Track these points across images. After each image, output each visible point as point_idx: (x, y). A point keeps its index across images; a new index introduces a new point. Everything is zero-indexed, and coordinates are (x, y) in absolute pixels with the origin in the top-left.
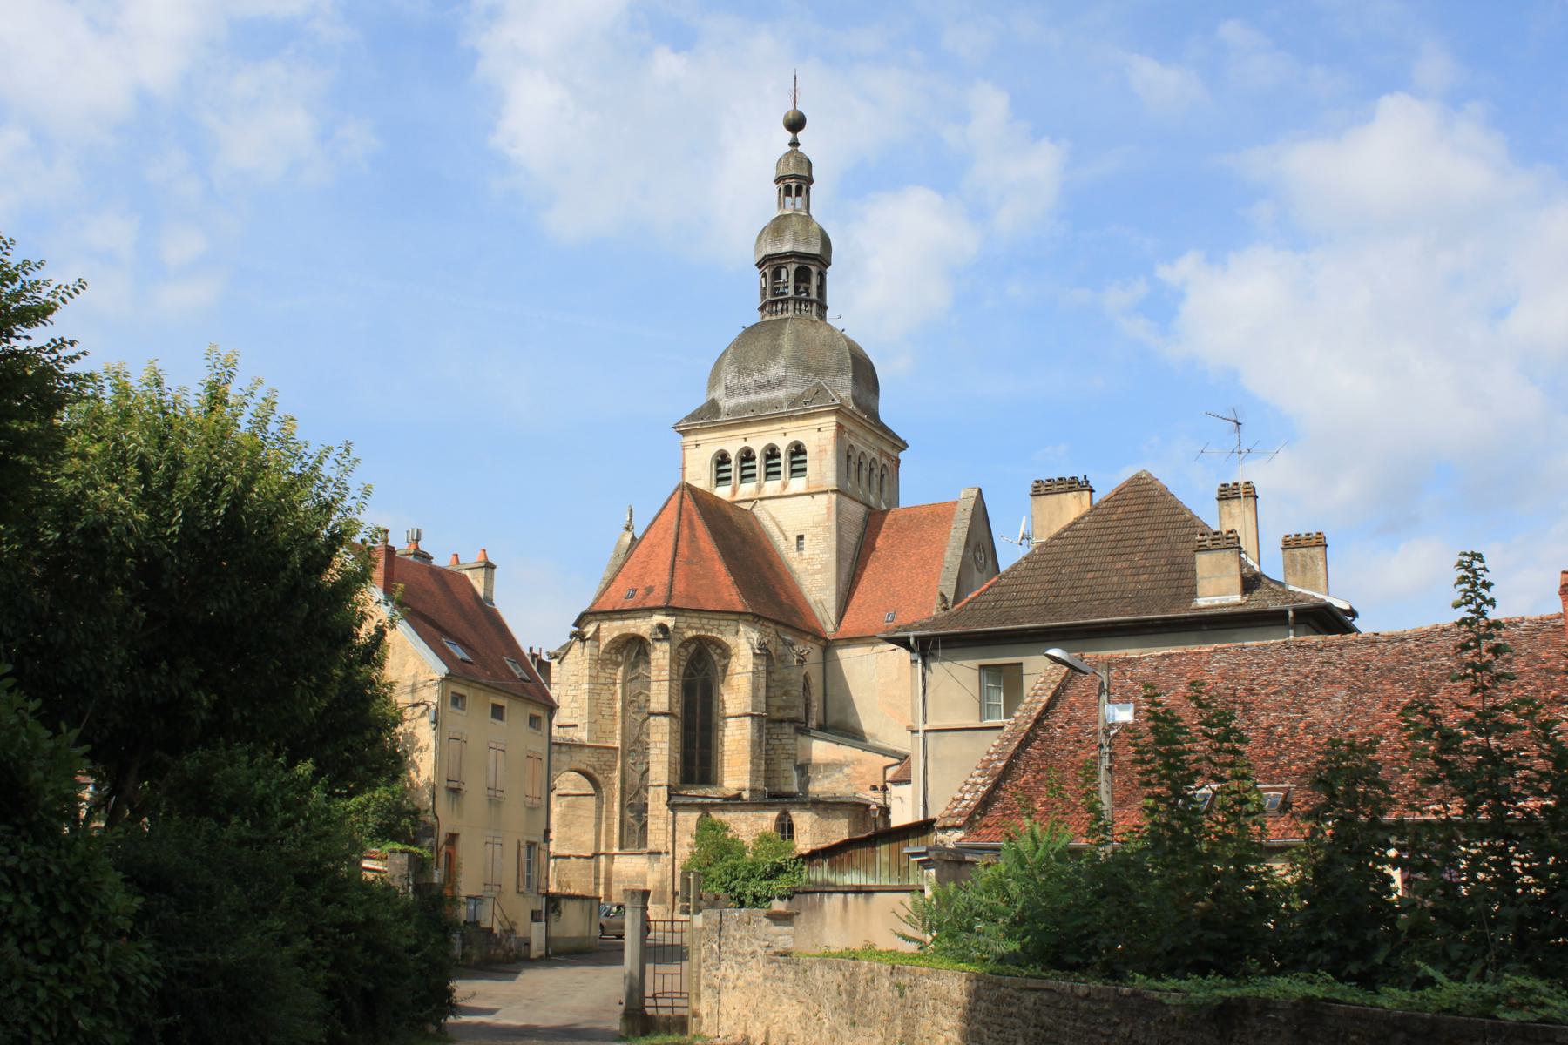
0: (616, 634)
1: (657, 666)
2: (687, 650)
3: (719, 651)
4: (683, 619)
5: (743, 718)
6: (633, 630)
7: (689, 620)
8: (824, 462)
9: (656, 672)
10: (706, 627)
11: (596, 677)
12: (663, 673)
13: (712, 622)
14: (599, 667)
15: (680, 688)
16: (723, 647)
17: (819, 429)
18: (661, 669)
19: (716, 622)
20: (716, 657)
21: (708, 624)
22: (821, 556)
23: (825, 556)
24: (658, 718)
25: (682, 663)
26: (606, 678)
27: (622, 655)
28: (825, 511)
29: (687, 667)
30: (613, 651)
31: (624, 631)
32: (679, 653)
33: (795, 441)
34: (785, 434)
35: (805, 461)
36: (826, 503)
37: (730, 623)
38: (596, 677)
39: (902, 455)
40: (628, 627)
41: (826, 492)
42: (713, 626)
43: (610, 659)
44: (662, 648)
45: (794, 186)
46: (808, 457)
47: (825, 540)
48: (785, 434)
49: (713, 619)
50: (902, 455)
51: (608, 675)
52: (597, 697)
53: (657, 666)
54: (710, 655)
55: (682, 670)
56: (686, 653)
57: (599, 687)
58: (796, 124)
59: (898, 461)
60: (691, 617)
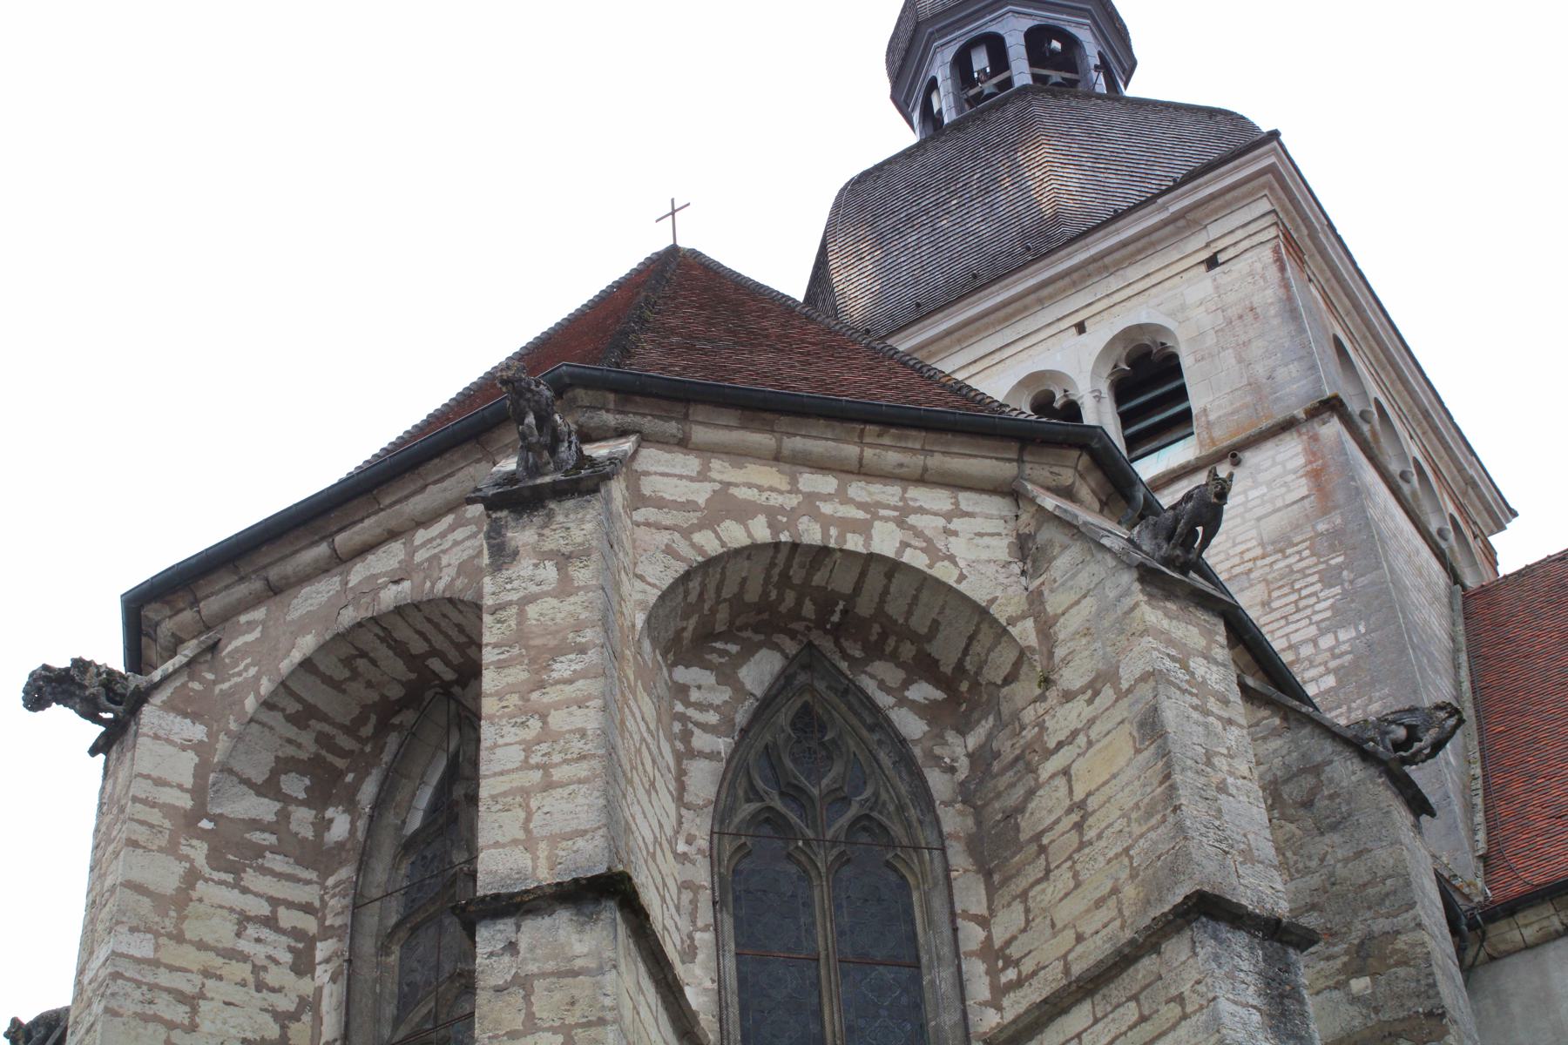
0: (306, 644)
1: (521, 636)
2: (727, 676)
3: (922, 691)
4: (689, 463)
5: (1147, 966)
6: (390, 596)
7: (721, 469)
8: (1257, 348)
9: (518, 674)
10: (826, 508)
11: (182, 899)
12: (562, 668)
13: (859, 490)
14: (198, 852)
15: (701, 874)
16: (946, 652)
17: (1212, 263)
18: (541, 659)
19: (889, 493)
20: (911, 726)
21: (842, 496)
22: (1327, 642)
23: (1344, 635)
24: (533, 932)
25: (701, 740)
26: (244, 919)
27: (351, 806)
28: (1302, 488)
29: (736, 777)
30: (295, 785)
31: (349, 617)
32: (681, 691)
33: (1127, 333)
34: (1081, 328)
35: (1181, 394)
36: (1301, 460)
37: (967, 500)
38: (182, 899)
39: (1494, 540)
40: (372, 588)
41: (1287, 426)
42: (871, 508)
43: (280, 825)
44: (554, 540)
46: (1186, 362)
47: (1329, 578)
48: (1081, 328)
49: (862, 471)
51: (263, 909)
52: (179, 1013)
53: (521, 636)
54: (880, 723)
55: (703, 780)
56: (723, 695)
57: (192, 958)
60: (739, 455)
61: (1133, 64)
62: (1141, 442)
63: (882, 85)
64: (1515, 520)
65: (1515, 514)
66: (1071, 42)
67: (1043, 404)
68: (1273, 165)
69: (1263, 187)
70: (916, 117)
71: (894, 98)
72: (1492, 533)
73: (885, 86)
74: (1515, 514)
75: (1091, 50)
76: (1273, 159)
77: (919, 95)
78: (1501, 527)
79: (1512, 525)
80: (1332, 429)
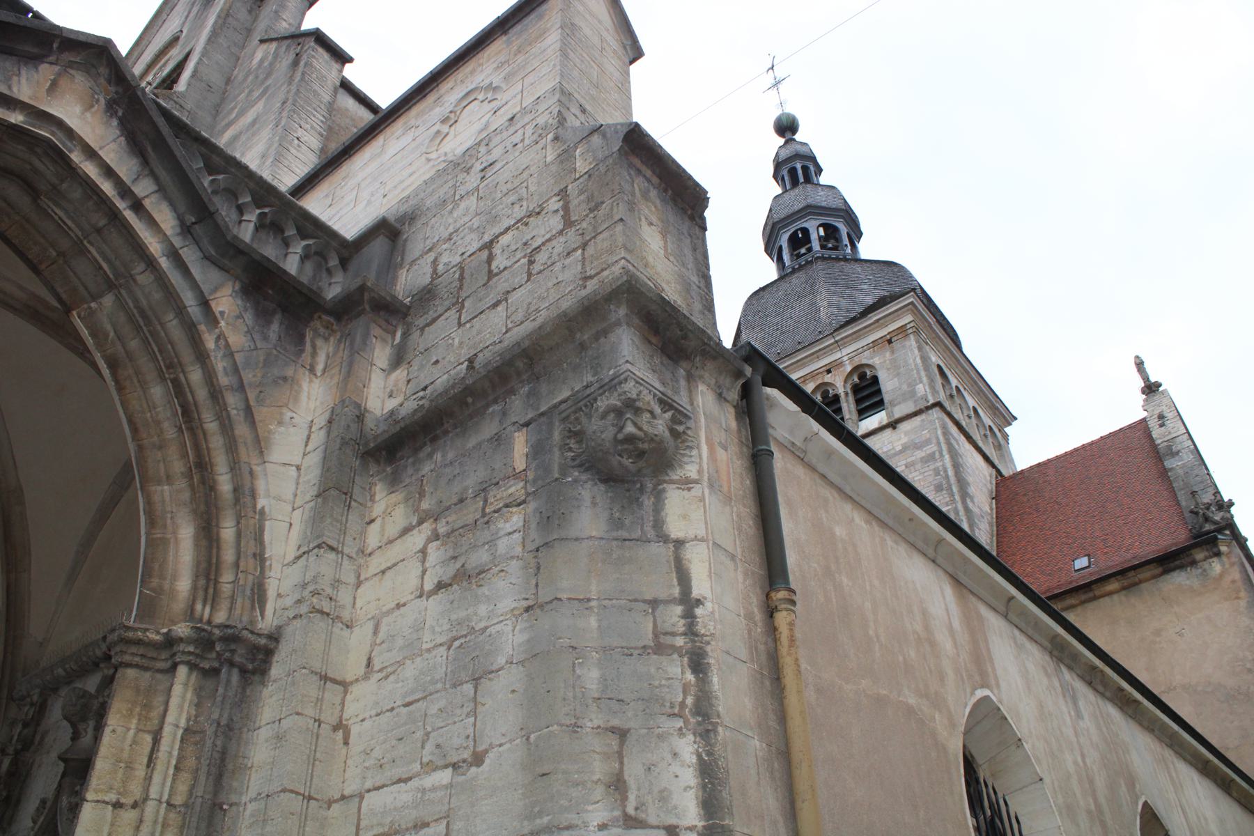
35: (879, 391)
39: (1007, 430)
45: (799, 166)
50: (1007, 430)
58: (786, 127)
59: (1006, 437)
61: (861, 234)
62: (863, 413)
63: (761, 246)
64: (1016, 421)
65: (1015, 418)
66: (836, 229)
67: (825, 395)
68: (912, 303)
69: (908, 310)
70: (775, 259)
71: (766, 251)
72: (1006, 427)
73: (762, 247)
74: (1015, 418)
75: (844, 230)
76: (912, 300)
77: (776, 250)
78: (1010, 424)
79: (1015, 423)
80: (936, 413)
